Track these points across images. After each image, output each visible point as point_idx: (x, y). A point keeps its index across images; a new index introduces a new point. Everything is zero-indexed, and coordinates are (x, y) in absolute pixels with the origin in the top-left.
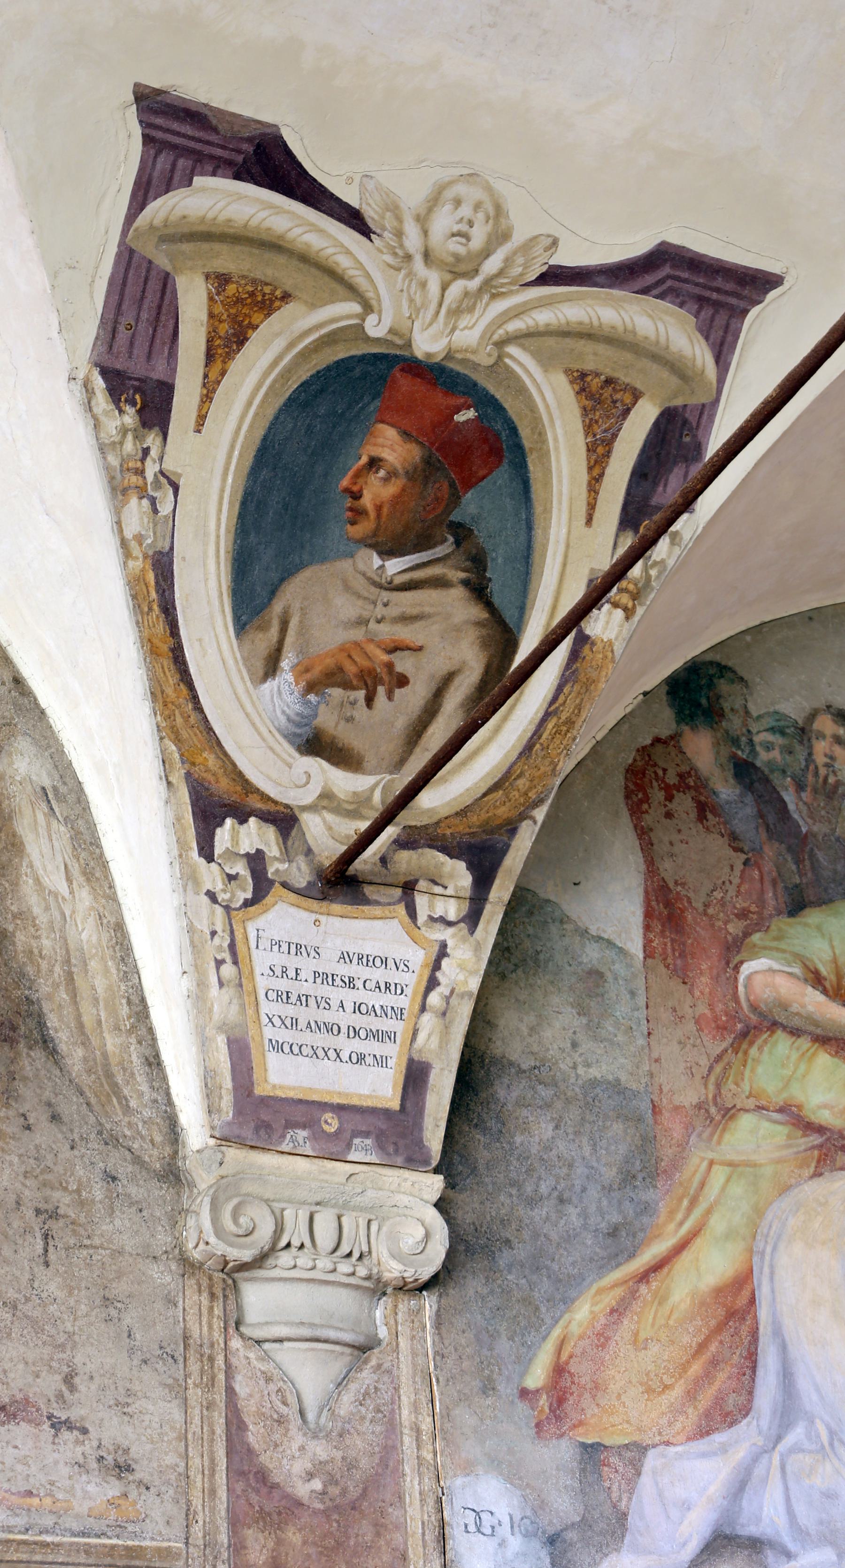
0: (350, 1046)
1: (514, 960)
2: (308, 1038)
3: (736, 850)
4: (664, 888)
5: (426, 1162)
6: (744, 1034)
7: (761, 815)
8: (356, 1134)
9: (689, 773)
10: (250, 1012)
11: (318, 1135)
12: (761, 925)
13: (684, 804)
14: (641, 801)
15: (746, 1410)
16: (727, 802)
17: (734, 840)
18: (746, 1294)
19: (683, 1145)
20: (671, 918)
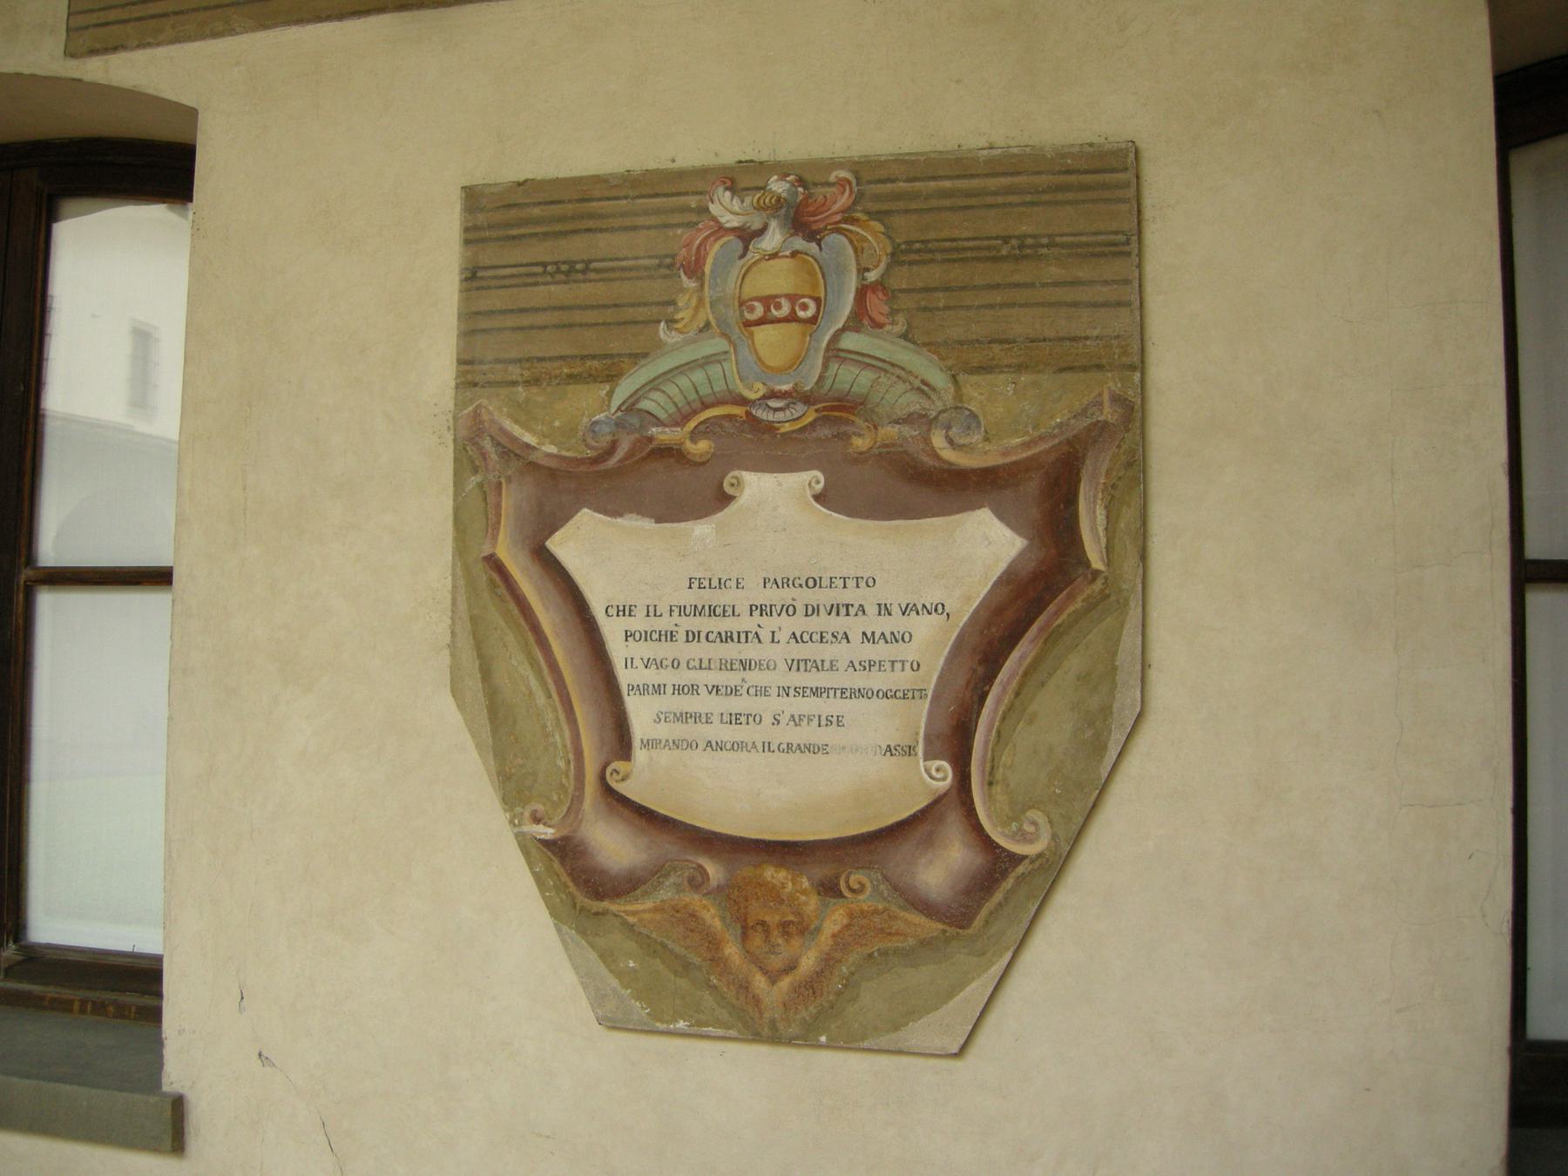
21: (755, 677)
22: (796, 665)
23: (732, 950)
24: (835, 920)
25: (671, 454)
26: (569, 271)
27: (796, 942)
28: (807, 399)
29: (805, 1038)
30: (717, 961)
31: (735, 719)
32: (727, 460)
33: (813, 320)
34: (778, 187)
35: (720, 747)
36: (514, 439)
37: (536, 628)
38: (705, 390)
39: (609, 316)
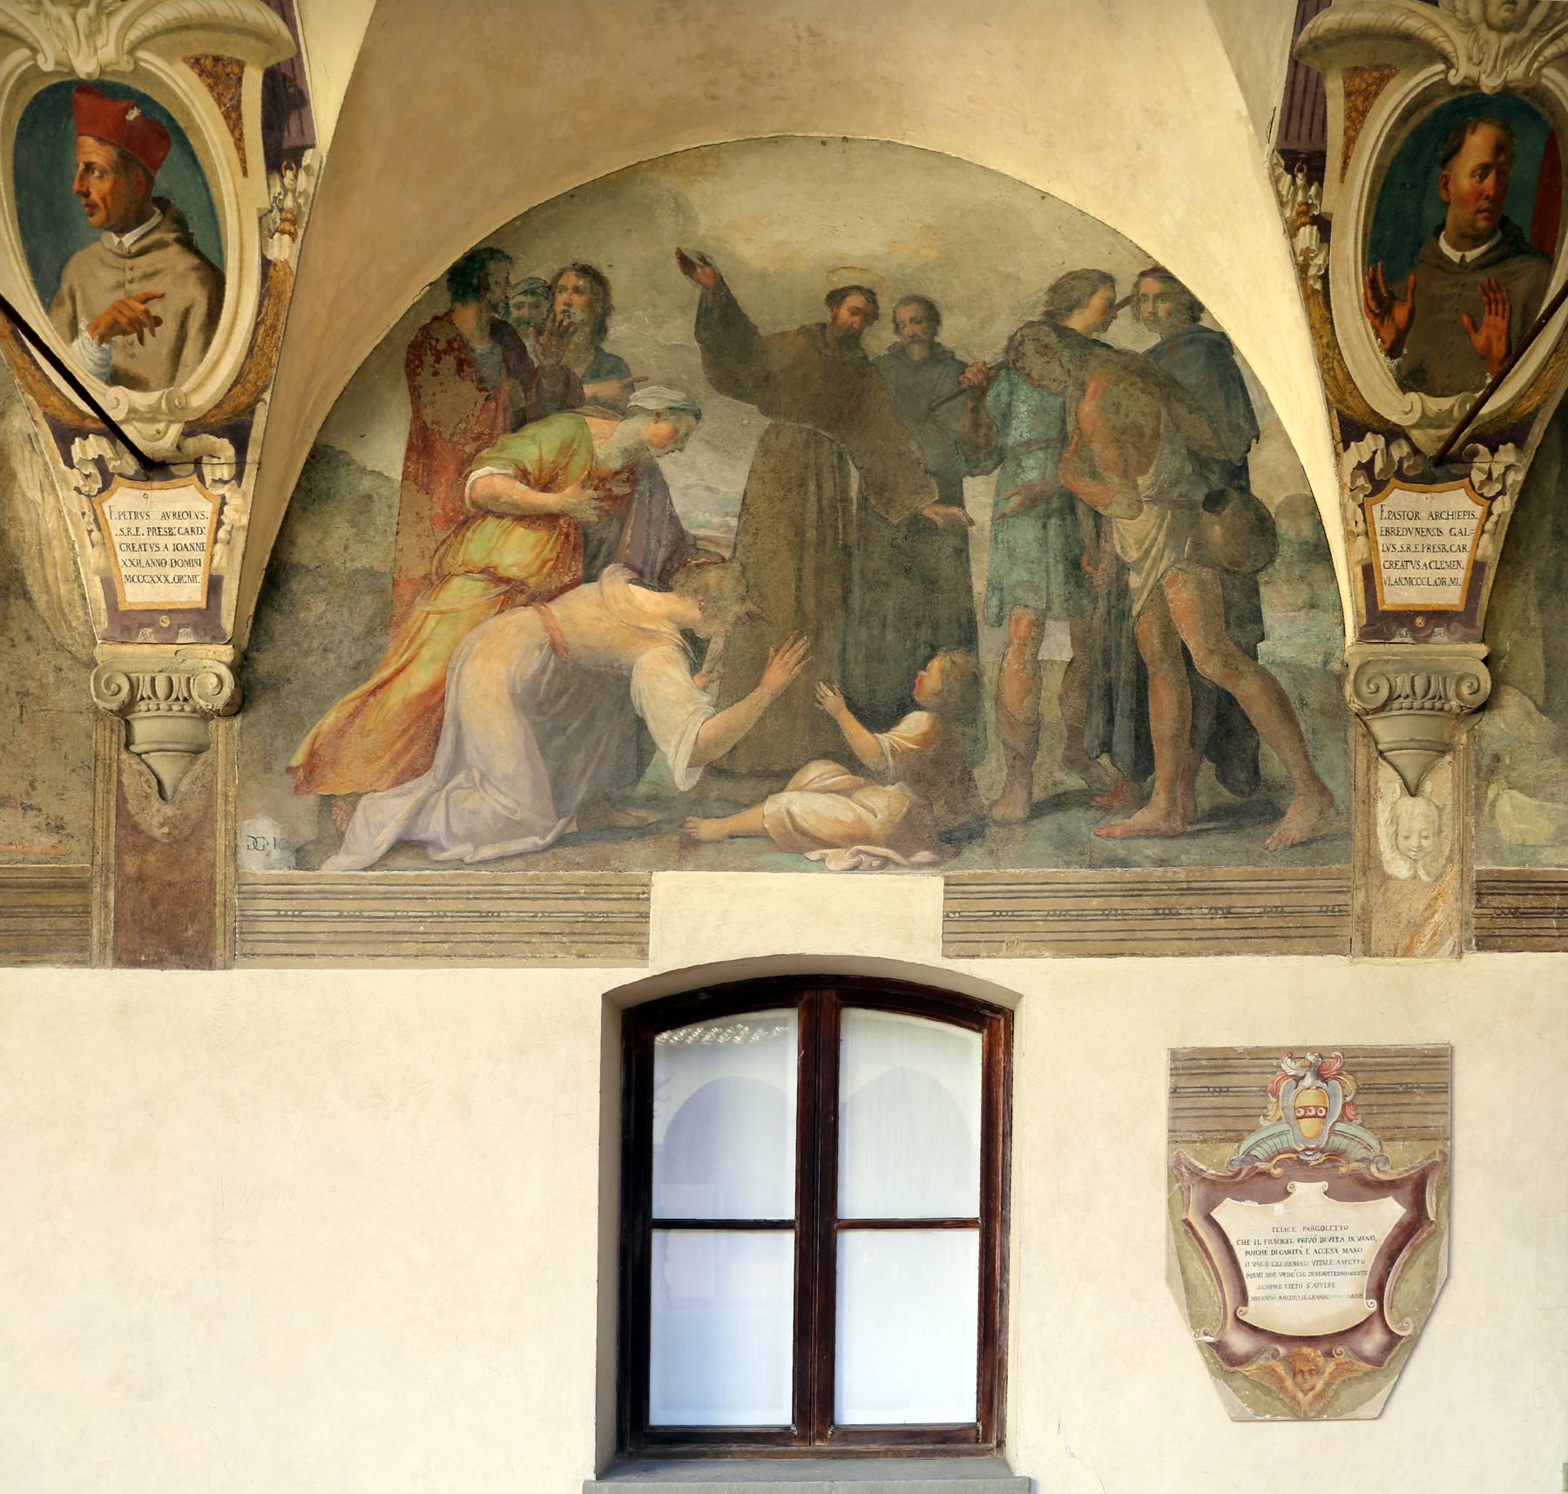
0: (172, 572)
1: (313, 497)
2: (147, 571)
3: (481, 390)
4: (425, 427)
5: (224, 638)
6: (465, 523)
7: (505, 360)
8: (180, 627)
9: (455, 340)
10: (112, 559)
11: (159, 630)
12: (490, 443)
13: (449, 362)
14: (417, 367)
15: (427, 767)
16: (481, 355)
17: (481, 384)
18: (438, 695)
19: (410, 604)
20: (424, 449)
21: (1300, 1269)
22: (1316, 1263)
23: (1289, 1383)
24: (1330, 1367)
25: (1264, 1174)
26: (1220, 1091)
27: (1315, 1377)
28: (1322, 1151)
29: (1318, 1417)
30: (1282, 1388)
31: (1292, 1286)
32: (1288, 1177)
33: (1324, 1117)
34: (1311, 1058)
35: (1285, 1298)
36: (1196, 1167)
37: (1206, 1251)
38: (1279, 1147)
39: (1238, 1113)
